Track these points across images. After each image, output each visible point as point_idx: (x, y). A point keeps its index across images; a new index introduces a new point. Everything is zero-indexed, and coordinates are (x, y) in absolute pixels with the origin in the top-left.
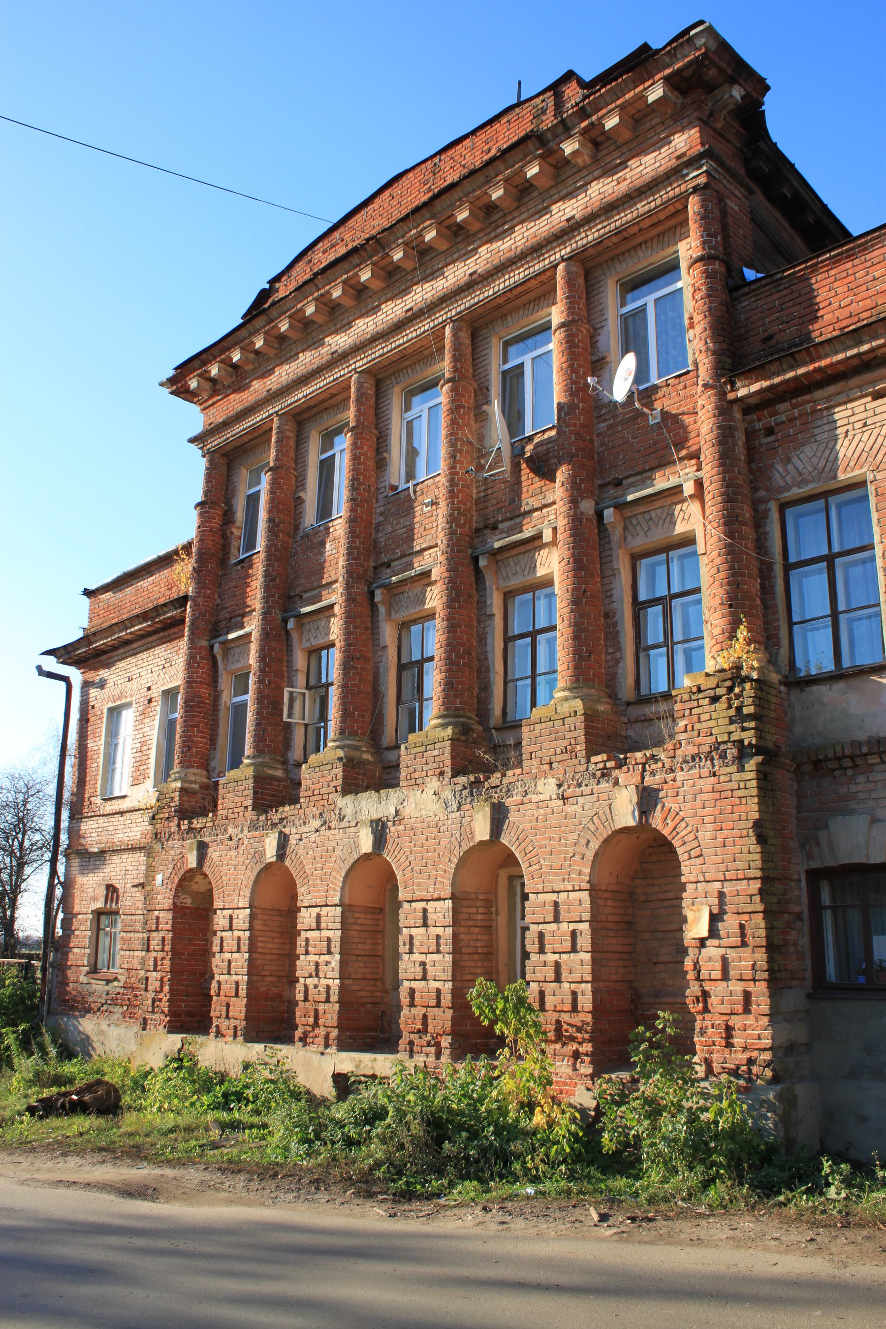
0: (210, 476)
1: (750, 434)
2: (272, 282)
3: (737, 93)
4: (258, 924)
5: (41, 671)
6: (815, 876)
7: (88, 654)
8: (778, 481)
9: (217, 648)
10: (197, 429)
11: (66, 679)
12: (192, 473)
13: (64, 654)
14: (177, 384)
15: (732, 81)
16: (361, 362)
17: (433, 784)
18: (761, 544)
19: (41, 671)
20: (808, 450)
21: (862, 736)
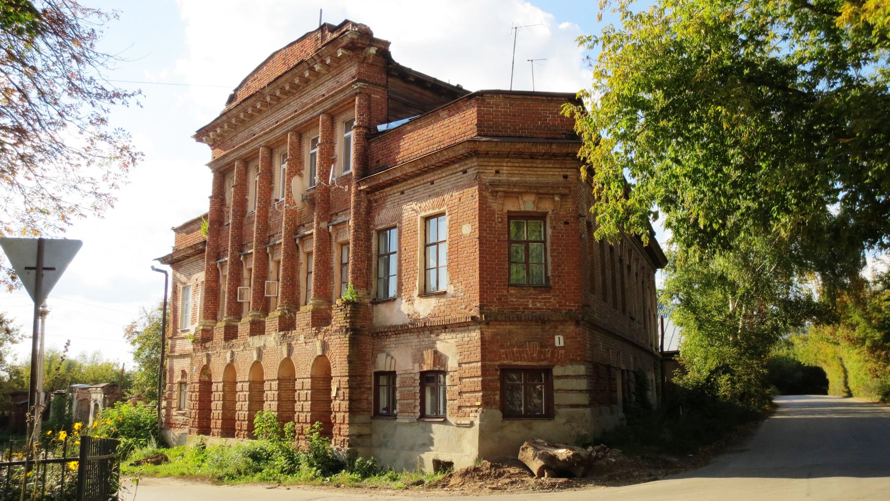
0: (215, 183)
1: (370, 202)
2: (236, 90)
3: (373, 50)
4: (227, 389)
5: (153, 268)
6: (378, 374)
7: (175, 260)
8: (376, 223)
9: (218, 265)
10: (210, 159)
11: (165, 272)
12: (207, 179)
13: (164, 260)
14: (201, 135)
15: (370, 46)
16: (262, 142)
17: (274, 334)
18: (368, 248)
19: (153, 268)
20: (384, 211)
21: (388, 324)
